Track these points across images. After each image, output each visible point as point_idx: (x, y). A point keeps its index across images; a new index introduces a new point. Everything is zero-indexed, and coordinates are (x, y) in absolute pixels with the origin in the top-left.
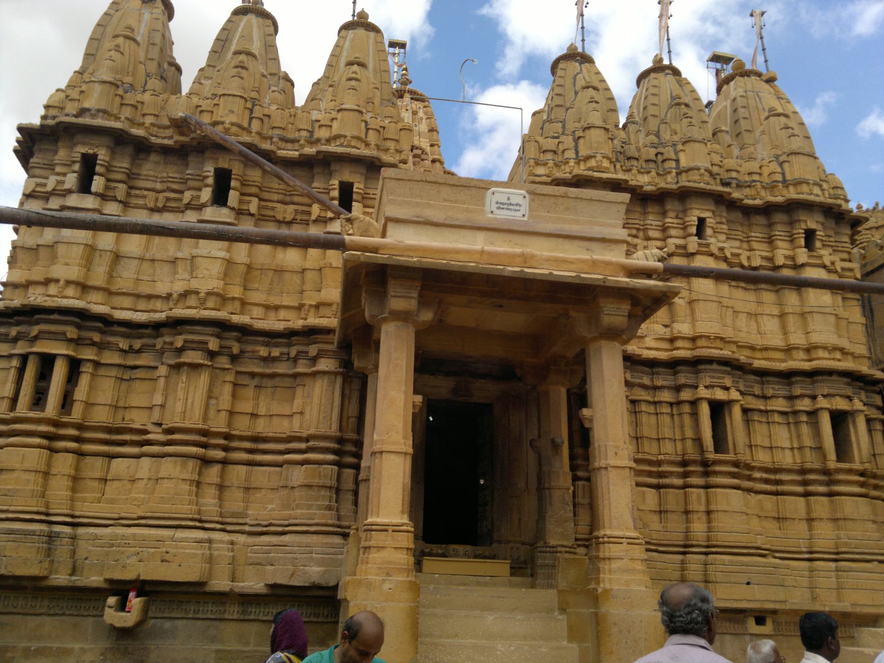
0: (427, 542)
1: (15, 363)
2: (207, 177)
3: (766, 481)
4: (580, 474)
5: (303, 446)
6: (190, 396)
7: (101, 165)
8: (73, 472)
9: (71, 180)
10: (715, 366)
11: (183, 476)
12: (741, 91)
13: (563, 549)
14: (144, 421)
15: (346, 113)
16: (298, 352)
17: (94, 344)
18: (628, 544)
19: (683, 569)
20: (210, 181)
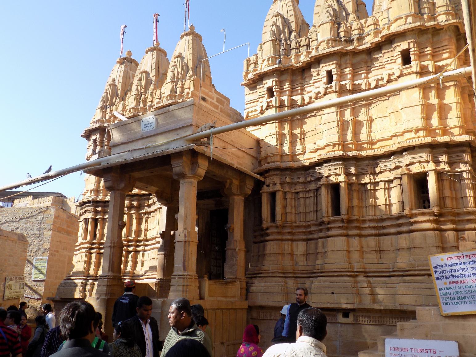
7: (98, 142)
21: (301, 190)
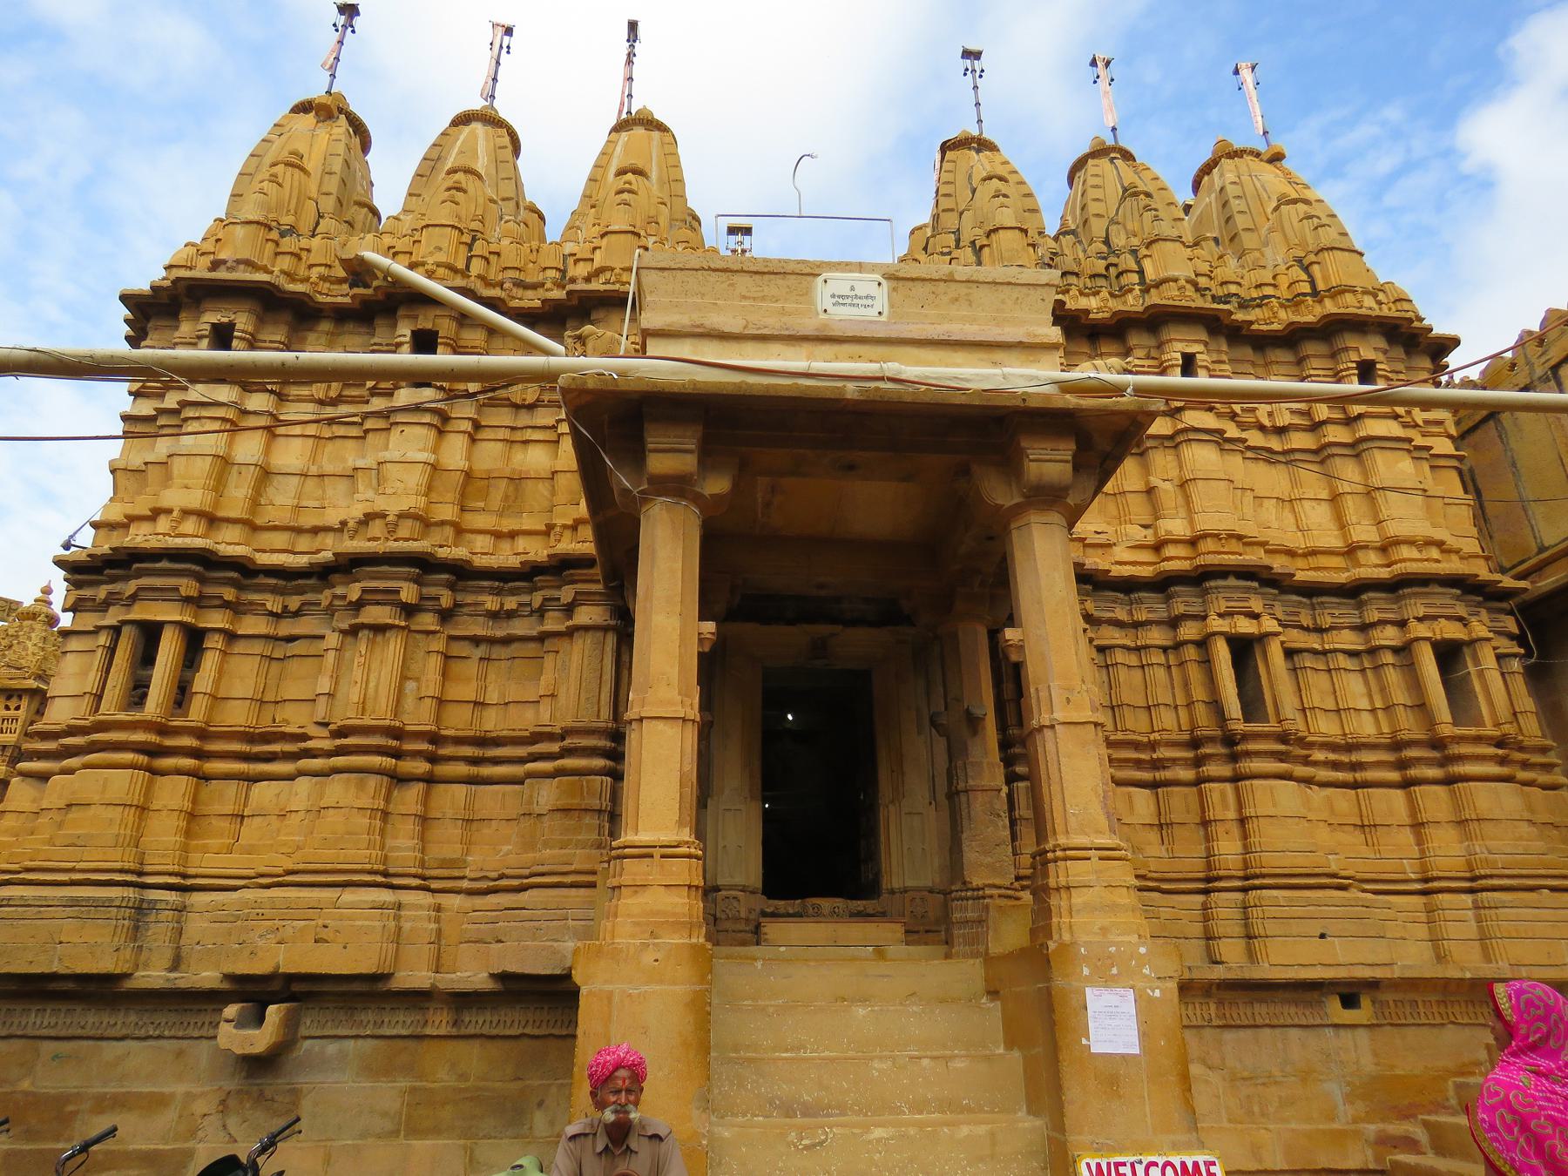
0: (769, 898)
1: (103, 639)
3: (1335, 766)
4: (1020, 769)
5: (555, 747)
8: (187, 805)
10: (1232, 581)
12: (1230, 177)
13: (995, 892)
14: (302, 722)
15: (613, 237)
16: (545, 599)
17: (226, 605)
18: (1101, 859)
19: (1206, 919)
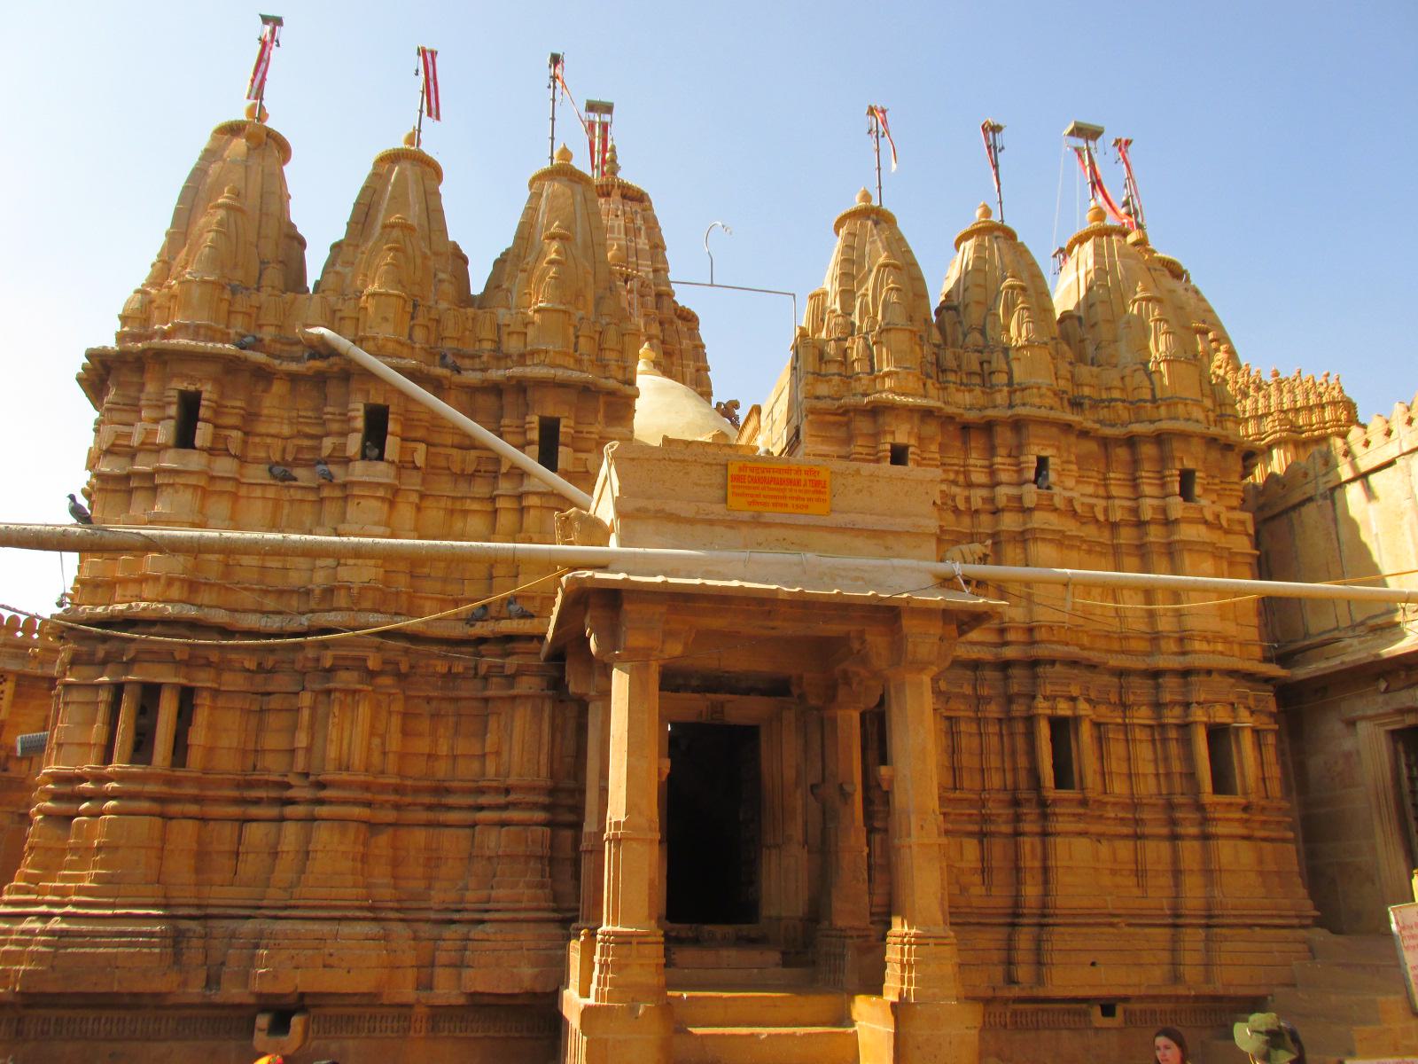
0: (671, 922)
1: (104, 696)
2: (354, 418)
4: (878, 824)
6: (346, 734)
9: (165, 433)
11: (342, 848)
18: (935, 944)
20: (360, 424)
21: (962, 714)
